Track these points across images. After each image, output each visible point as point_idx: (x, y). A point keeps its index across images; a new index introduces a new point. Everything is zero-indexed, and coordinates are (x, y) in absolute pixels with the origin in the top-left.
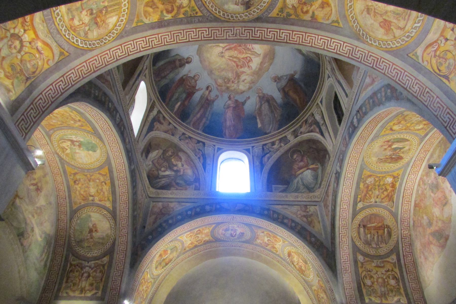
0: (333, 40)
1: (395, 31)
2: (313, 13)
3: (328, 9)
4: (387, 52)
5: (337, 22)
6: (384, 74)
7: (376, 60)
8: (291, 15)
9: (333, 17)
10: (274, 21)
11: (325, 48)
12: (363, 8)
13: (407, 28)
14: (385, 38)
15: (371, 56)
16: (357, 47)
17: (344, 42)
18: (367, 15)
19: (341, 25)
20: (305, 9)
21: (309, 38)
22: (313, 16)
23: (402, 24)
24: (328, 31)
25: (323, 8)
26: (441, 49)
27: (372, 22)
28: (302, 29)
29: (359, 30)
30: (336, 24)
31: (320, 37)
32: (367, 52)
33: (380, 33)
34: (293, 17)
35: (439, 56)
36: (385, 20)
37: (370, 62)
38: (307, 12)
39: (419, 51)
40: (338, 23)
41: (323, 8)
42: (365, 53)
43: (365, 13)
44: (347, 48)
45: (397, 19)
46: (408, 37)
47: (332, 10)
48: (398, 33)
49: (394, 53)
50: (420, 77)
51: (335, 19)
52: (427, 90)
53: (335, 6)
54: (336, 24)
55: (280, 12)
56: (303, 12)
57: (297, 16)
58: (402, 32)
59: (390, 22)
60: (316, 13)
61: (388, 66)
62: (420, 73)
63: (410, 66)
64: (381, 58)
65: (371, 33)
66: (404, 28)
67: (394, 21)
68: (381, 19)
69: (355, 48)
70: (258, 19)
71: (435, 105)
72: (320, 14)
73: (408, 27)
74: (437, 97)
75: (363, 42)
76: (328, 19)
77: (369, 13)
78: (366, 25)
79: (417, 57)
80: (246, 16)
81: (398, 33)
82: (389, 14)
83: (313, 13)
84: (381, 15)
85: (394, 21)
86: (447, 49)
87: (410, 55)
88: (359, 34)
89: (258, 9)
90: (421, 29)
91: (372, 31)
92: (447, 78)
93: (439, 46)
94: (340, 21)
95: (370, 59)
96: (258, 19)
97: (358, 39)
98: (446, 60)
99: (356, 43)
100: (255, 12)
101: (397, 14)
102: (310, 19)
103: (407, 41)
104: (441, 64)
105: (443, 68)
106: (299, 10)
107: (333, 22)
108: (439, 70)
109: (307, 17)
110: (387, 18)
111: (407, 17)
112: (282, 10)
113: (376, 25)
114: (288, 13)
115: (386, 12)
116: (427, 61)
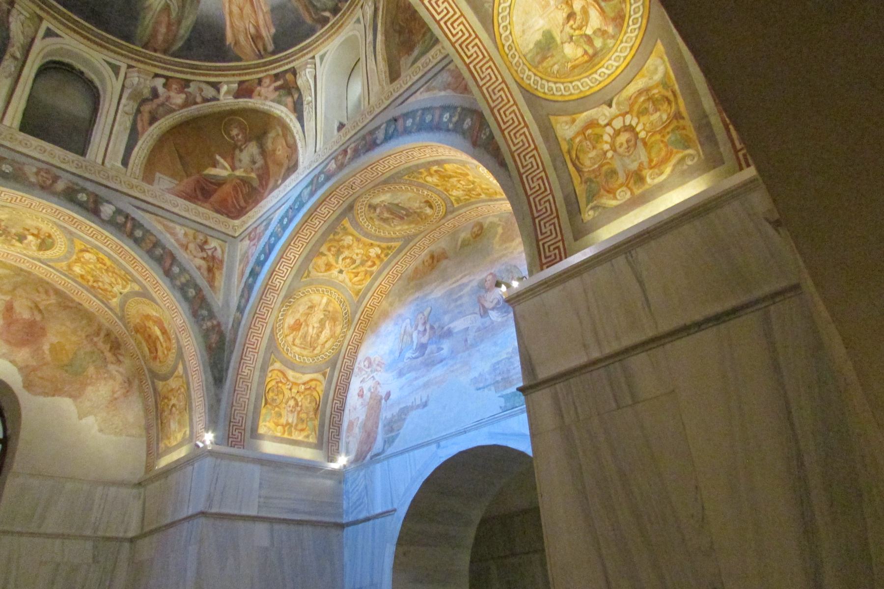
0: (290, 269)
1: (292, 335)
2: (325, 255)
3: (323, 269)
4: (273, 328)
5: (308, 276)
6: (250, 328)
7: (265, 317)
8: (334, 235)
9: (314, 273)
10: (339, 219)
11: (282, 260)
12: (314, 302)
13: (294, 347)
14: (286, 326)
15: (268, 311)
16: (278, 295)
17: (285, 281)
18: (307, 307)
19: (303, 280)
20: (333, 249)
21: (301, 245)
22: (323, 254)
23: (297, 341)
24: (300, 266)
25: (326, 265)
26: (283, 387)
27: (301, 312)
28: (313, 241)
29: (294, 298)
30: (305, 275)
31: (297, 256)
32: (272, 306)
33: (290, 321)
34: (331, 236)
35: (278, 387)
36: (301, 324)
37: (262, 310)
38: (329, 250)
39: (278, 365)
40: (306, 277)
41: (326, 265)
42: (271, 305)
43: (310, 304)
44: (278, 284)
45: (301, 336)
46: (287, 350)
47: (321, 272)
48: (290, 339)
49: (272, 338)
50: (257, 373)
51: (311, 275)
52: (249, 384)
53: (323, 276)
54: (305, 275)
55: (344, 227)
56: (332, 246)
57: (331, 240)
58: (290, 343)
59: (299, 329)
60: (324, 258)
61: (260, 332)
62: (261, 371)
63: (264, 359)
64: (267, 323)
65: (290, 311)
66: (294, 345)
67: (300, 334)
68: (302, 320)
69: (278, 292)
70: (351, 208)
71: (241, 399)
72: (321, 261)
73: (297, 349)
74: (248, 399)
75: (283, 302)
76: (313, 268)
77: (309, 308)
78: (299, 305)
79: (272, 364)
80: (363, 201)
81: (290, 339)
82: (306, 328)
83: (325, 255)
84: (305, 321)
85: (300, 334)
86: (285, 393)
87: (273, 356)
88: (291, 298)
89: (361, 212)
90: (295, 361)
91: (292, 312)
92: (266, 404)
93: (285, 384)
94: (308, 279)
95: (264, 311)
96: (351, 208)
97: (286, 297)
98: (277, 395)
99: (283, 294)
100: (360, 209)
101: (305, 337)
102: (321, 251)
103: (283, 349)
104: (273, 391)
105: (271, 395)
106: (335, 244)
107: (309, 272)
108: (268, 392)
109: (324, 249)
110: (303, 326)
111: (303, 346)
112: (345, 229)
113: (298, 316)
114: (339, 233)
115: (307, 325)
116: (271, 376)
